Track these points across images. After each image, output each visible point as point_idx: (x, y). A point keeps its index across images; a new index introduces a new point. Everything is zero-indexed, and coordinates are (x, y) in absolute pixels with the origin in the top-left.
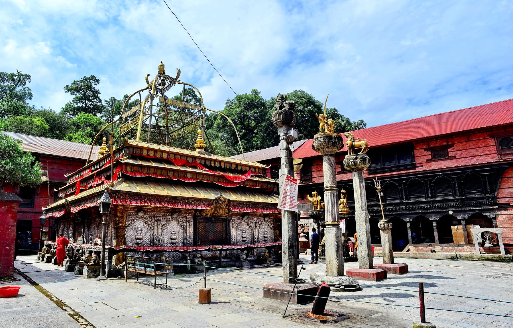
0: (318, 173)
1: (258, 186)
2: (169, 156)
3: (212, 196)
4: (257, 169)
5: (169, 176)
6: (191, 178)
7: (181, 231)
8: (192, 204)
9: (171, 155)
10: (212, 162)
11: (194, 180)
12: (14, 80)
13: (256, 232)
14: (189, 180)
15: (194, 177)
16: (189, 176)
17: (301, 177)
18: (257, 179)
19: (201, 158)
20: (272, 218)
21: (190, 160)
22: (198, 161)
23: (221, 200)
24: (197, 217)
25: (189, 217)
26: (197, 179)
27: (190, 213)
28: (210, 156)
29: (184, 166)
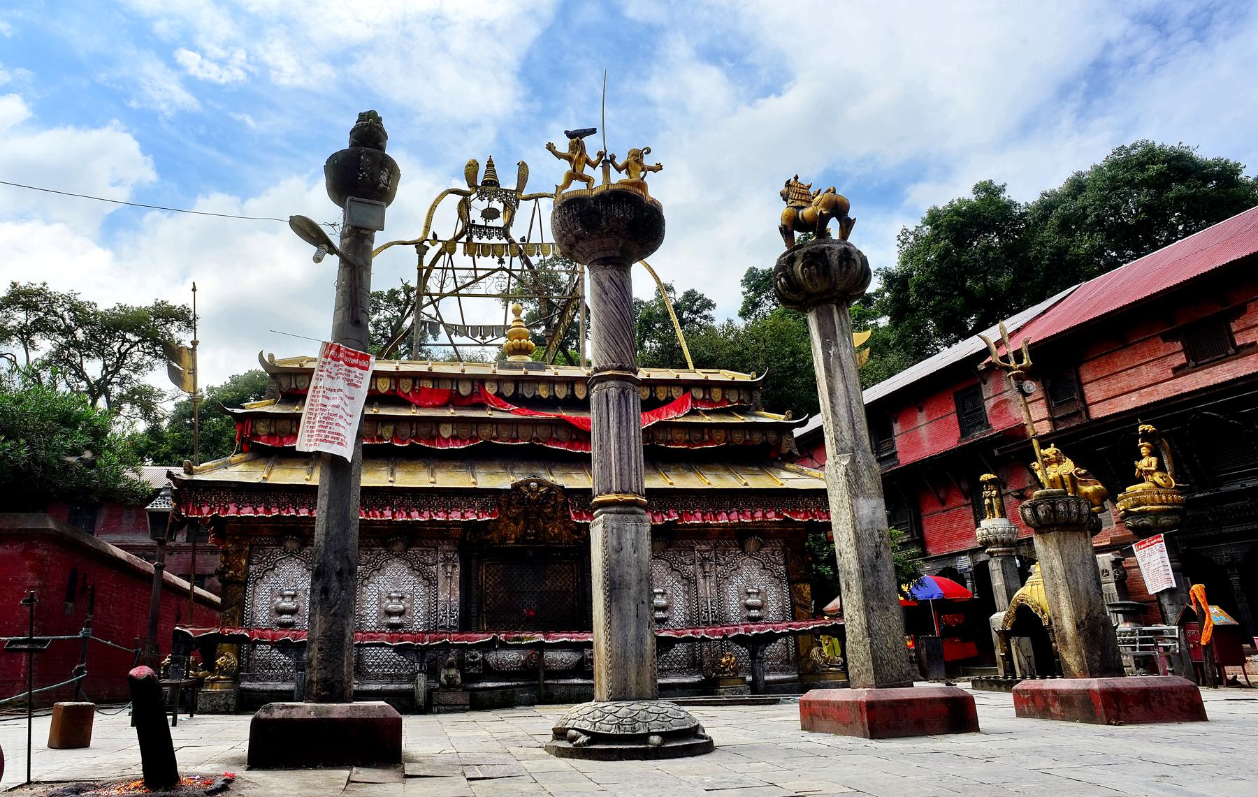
0: (1104, 385)
1: (711, 441)
2: (397, 384)
3: (502, 481)
4: (717, 394)
5: (381, 438)
6: (454, 438)
7: (420, 590)
8: (431, 507)
9: (402, 381)
10: (541, 387)
11: (463, 442)
12: (398, 303)
13: (706, 588)
14: (447, 441)
15: (465, 431)
16: (446, 432)
17: (1049, 410)
18: (707, 419)
19: (499, 380)
20: (778, 544)
21: (465, 390)
22: (491, 389)
23: (530, 490)
24: (471, 547)
25: (446, 547)
26: (472, 439)
27: (447, 538)
28: (543, 369)
29: (445, 406)
